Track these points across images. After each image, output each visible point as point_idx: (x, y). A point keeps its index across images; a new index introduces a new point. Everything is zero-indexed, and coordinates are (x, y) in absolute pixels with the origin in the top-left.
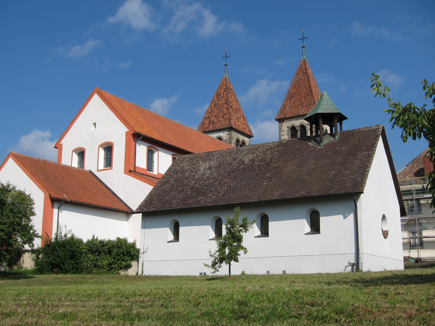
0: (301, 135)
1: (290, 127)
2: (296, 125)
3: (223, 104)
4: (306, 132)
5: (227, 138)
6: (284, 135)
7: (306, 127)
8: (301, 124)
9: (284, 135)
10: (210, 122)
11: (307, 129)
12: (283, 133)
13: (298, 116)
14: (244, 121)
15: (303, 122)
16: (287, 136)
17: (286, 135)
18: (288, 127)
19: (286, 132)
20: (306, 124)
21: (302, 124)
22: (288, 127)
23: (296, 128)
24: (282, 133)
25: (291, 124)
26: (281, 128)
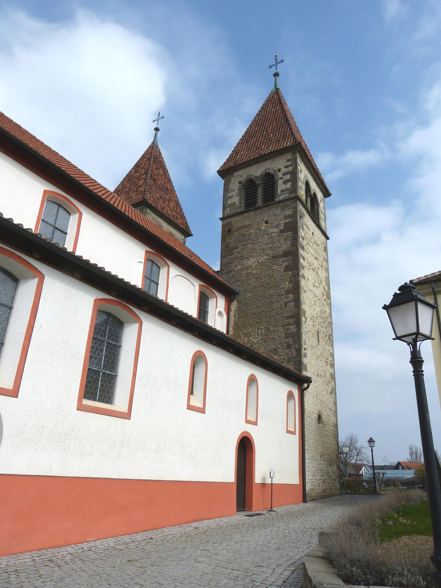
0: (264, 195)
2: (256, 176)
6: (232, 197)
9: (232, 197)
11: (276, 178)
12: (230, 195)
15: (269, 168)
16: (238, 198)
19: (237, 191)
20: (275, 171)
21: (268, 171)
22: (240, 183)
23: (255, 180)
24: (228, 195)
25: (247, 176)
26: (227, 186)
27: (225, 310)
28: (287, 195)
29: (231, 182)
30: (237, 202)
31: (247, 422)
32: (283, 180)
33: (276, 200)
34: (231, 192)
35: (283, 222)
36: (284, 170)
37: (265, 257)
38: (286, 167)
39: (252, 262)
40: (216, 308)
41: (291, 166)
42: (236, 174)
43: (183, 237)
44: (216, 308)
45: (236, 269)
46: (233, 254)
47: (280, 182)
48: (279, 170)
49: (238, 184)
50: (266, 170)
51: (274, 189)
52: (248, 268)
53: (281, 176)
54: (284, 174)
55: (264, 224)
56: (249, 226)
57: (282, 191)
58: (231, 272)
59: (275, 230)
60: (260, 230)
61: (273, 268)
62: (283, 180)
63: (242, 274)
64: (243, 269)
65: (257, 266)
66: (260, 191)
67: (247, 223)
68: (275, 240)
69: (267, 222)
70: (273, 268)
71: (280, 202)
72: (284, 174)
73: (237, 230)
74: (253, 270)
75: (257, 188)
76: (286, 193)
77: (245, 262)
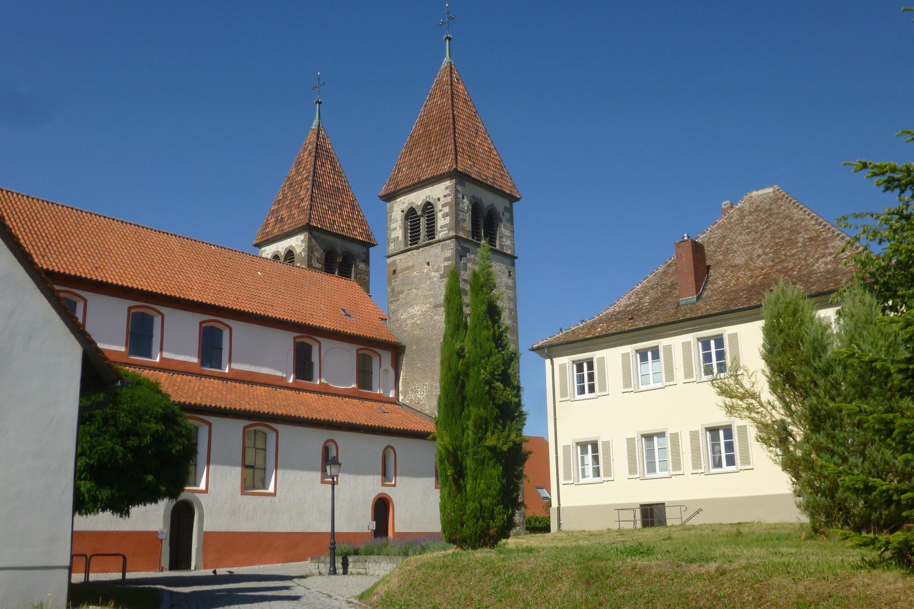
0: (427, 224)
1: (406, 211)
3: (302, 181)
4: (434, 219)
5: (302, 248)
6: (395, 229)
7: (434, 205)
8: (425, 202)
9: (395, 229)
10: (276, 221)
11: (436, 209)
13: (419, 183)
14: (353, 214)
16: (401, 231)
17: (398, 228)
18: (403, 211)
19: (400, 222)
20: (435, 200)
21: (428, 199)
22: (403, 211)
25: (409, 204)
27: (392, 366)
28: (445, 232)
29: (395, 208)
30: (401, 238)
31: (383, 485)
32: (443, 212)
33: (437, 238)
34: (394, 223)
35: (442, 265)
36: (443, 199)
37: (428, 305)
38: (445, 196)
39: (416, 310)
40: (380, 367)
41: (449, 195)
42: (398, 200)
43: (364, 250)
44: (380, 367)
45: (402, 317)
46: (399, 300)
47: (440, 215)
48: (439, 199)
49: (400, 214)
50: (426, 197)
51: (434, 222)
52: (413, 317)
53: (441, 208)
54: (443, 206)
55: (426, 266)
56: (413, 267)
57: (442, 227)
58: (397, 321)
59: (437, 274)
60: (423, 272)
61: (435, 318)
62: (443, 212)
63: (408, 324)
64: (409, 318)
65: (420, 315)
66: (423, 222)
67: (410, 264)
68: (436, 286)
69: (428, 264)
70: (435, 318)
71: (439, 241)
72: (443, 206)
73: (402, 271)
74: (417, 320)
75: (419, 219)
76: (445, 230)
77: (410, 310)
